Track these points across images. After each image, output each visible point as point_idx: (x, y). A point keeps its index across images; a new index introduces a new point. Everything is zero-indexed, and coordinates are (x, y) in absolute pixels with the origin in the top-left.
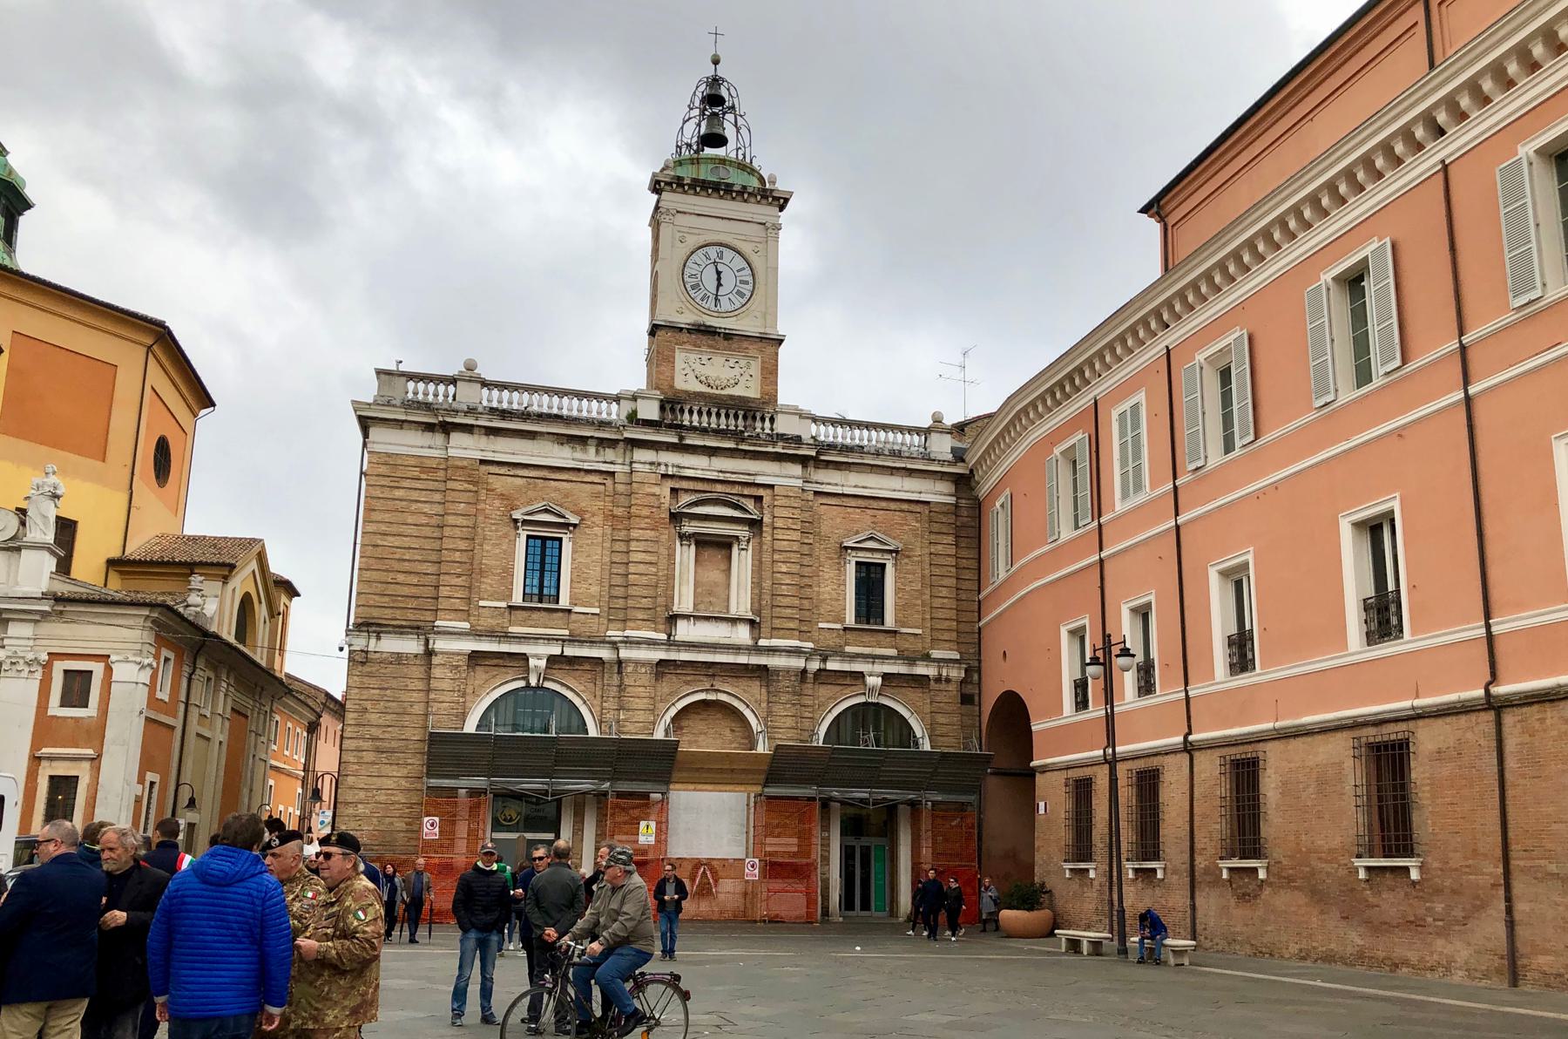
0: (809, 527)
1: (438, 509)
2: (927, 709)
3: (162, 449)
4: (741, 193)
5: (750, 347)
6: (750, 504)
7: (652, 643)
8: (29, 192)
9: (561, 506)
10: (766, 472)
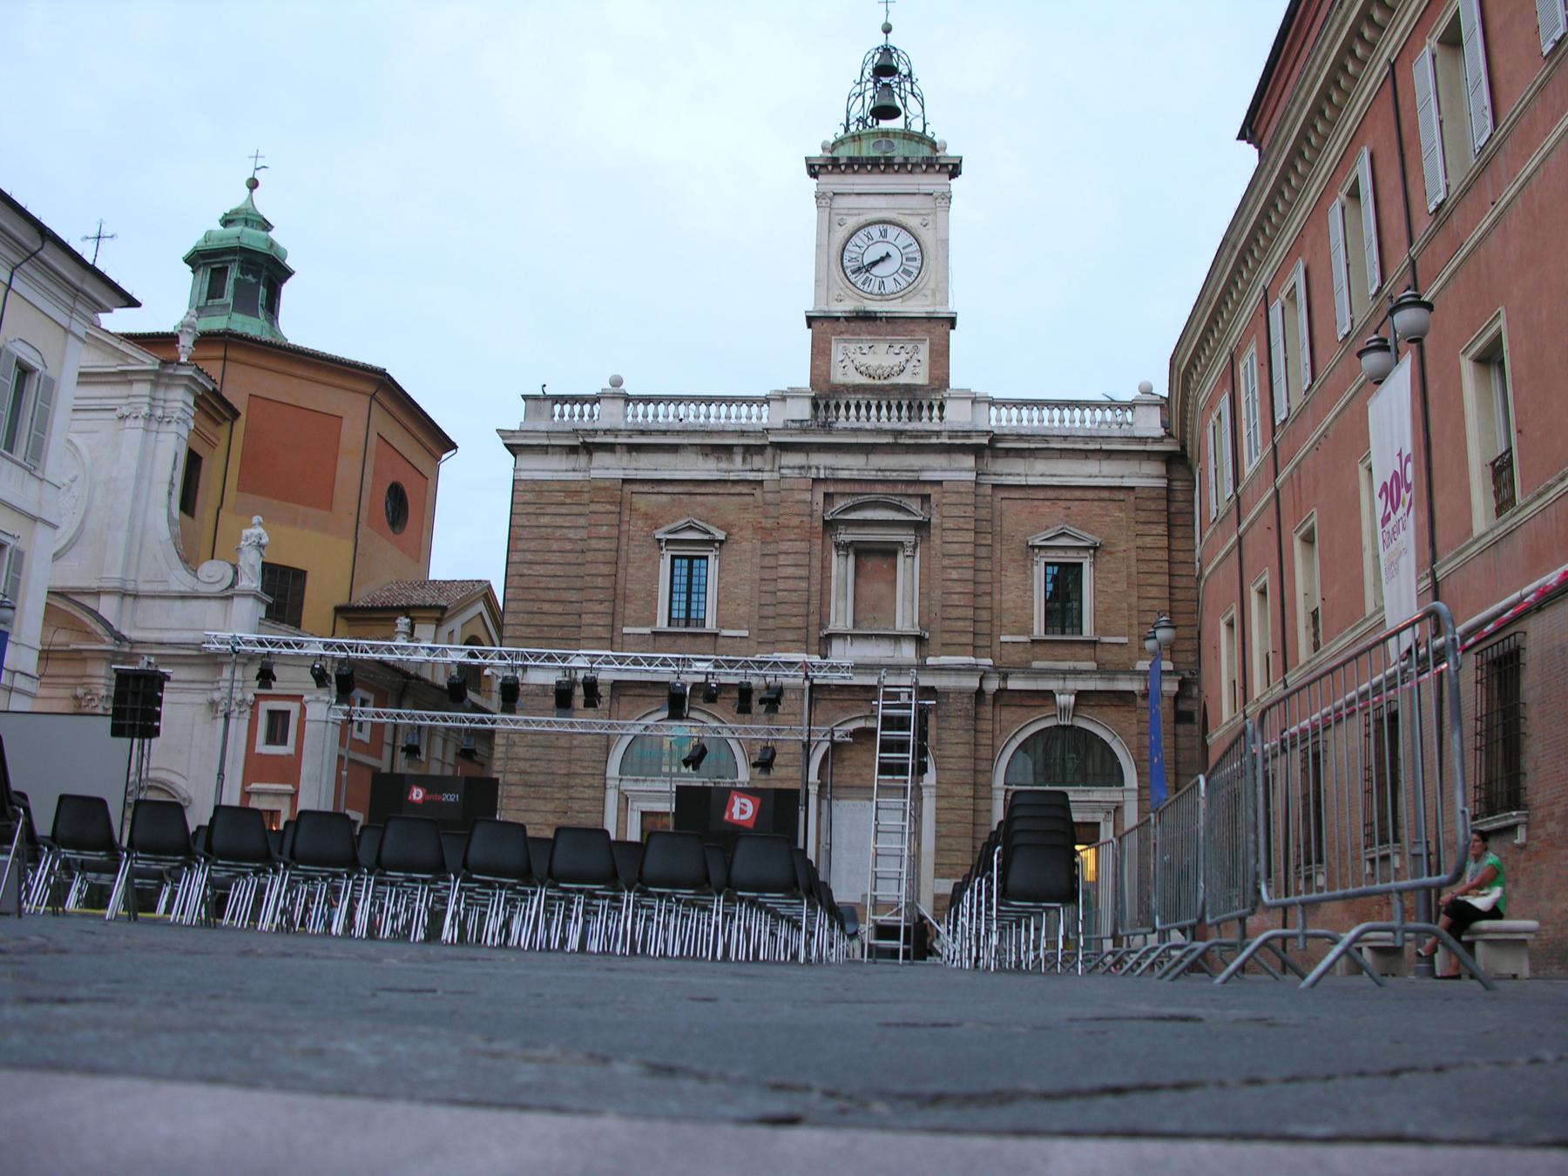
0: (984, 528)
1: (583, 534)
2: (1134, 729)
4: (903, 165)
5: (917, 329)
6: (915, 505)
8: (290, 262)
9: (707, 522)
10: (934, 468)
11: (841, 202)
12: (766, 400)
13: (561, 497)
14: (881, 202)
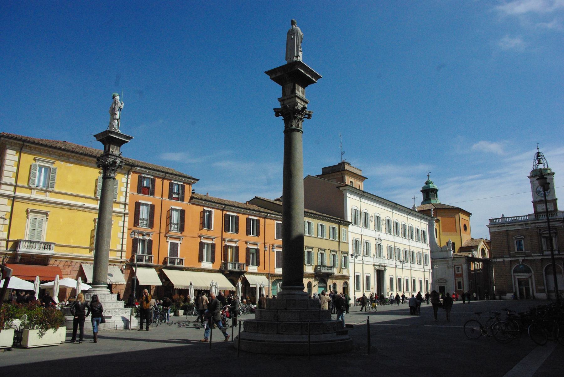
3: (465, 226)
7: (539, 256)
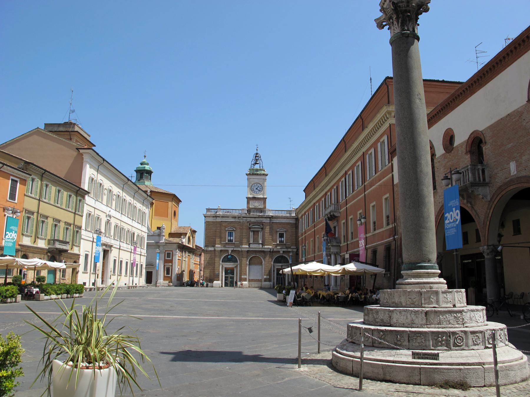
11: (251, 180)
12: (241, 210)
13: (212, 224)
14: (257, 180)
